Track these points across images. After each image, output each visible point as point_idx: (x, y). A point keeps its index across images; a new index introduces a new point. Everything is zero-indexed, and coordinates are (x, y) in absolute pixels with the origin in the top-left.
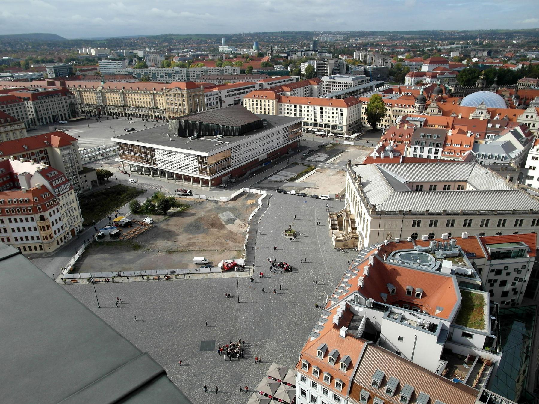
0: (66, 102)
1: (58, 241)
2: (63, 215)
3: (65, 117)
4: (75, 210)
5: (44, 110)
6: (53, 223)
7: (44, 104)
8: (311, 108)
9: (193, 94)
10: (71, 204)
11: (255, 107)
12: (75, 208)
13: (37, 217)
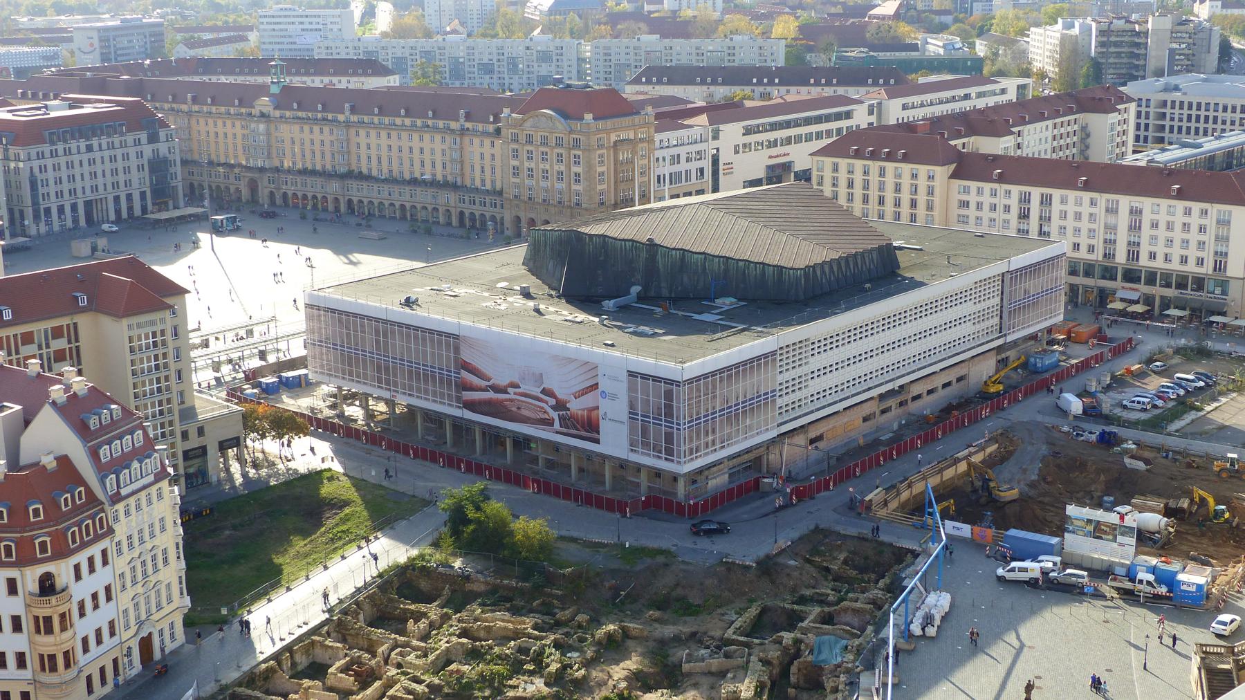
0: (140, 155)
1: (89, 679)
2: (122, 575)
3: (130, 209)
4: (166, 561)
5: (59, 181)
6: (82, 606)
7: (63, 160)
8: (1093, 203)
9: (613, 138)
10: (152, 536)
11: (858, 192)
12: (165, 551)
13: (29, 578)
